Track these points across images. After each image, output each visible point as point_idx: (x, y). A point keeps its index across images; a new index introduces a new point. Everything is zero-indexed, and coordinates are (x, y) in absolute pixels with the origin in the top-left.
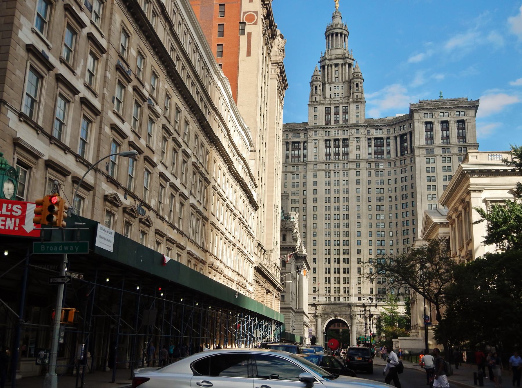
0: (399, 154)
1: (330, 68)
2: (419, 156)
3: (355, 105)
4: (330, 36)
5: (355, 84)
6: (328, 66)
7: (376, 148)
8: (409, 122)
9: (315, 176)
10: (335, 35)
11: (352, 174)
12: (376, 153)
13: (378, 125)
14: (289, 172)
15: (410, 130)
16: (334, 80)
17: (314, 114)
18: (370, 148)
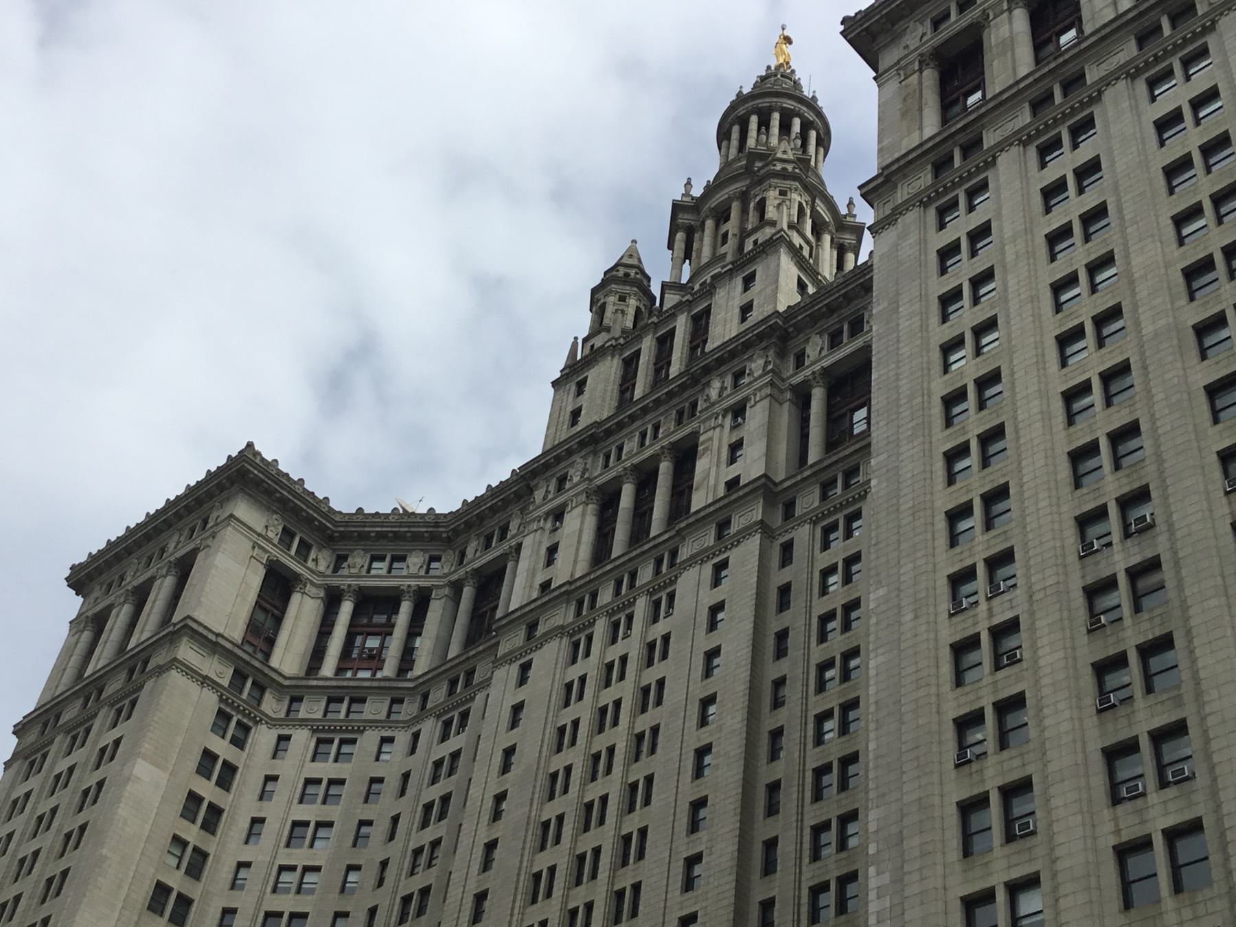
10: (736, 130)
17: (570, 409)
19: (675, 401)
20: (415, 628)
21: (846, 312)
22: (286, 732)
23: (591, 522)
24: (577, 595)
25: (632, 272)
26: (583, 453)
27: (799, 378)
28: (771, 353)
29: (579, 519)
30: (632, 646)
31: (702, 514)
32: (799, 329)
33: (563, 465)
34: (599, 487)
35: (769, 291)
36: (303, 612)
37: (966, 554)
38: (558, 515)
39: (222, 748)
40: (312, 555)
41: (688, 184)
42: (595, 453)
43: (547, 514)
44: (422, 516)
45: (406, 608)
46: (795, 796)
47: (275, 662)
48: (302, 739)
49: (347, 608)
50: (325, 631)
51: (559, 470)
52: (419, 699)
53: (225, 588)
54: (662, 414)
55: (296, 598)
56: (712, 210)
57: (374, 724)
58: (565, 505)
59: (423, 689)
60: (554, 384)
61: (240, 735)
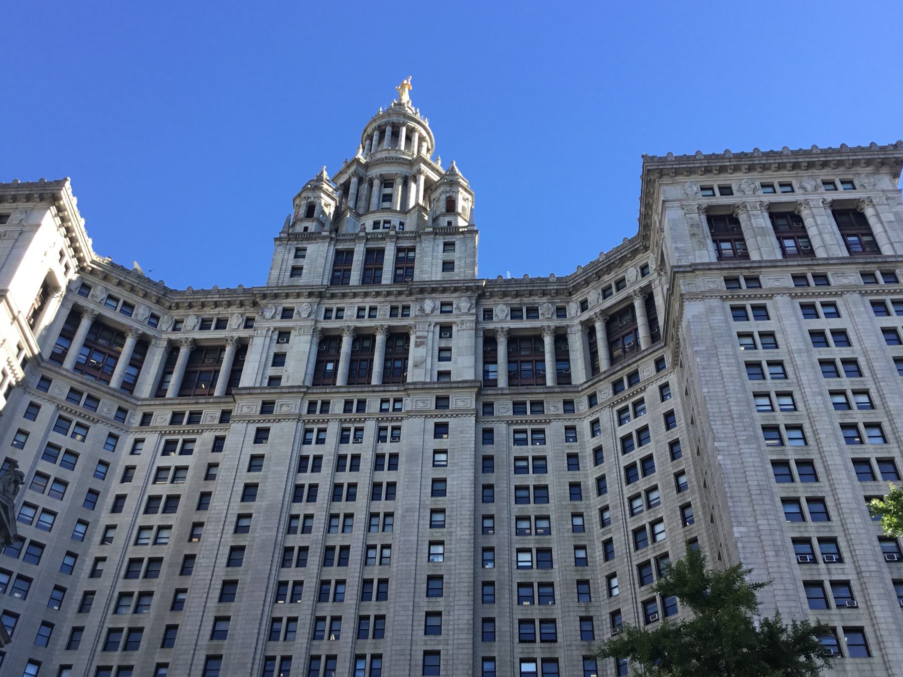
0: (603, 363)
1: (365, 186)
2: (702, 296)
3: (440, 241)
4: (376, 133)
5: (444, 197)
6: (361, 181)
7: (514, 367)
8: (640, 259)
9: (261, 435)
10: (389, 130)
11: (415, 434)
12: (512, 378)
13: (523, 293)
14: (155, 430)
15: (644, 283)
16: (373, 207)
17: (291, 262)
18: (491, 367)
19: (392, 298)
20: (137, 362)
21: (526, 300)
22: (37, 401)
24: (313, 397)
26: (310, 300)
27: (490, 326)
28: (474, 301)
29: (309, 345)
30: (366, 449)
31: (428, 386)
32: (492, 295)
33: (291, 300)
34: (323, 330)
35: (469, 260)
37: (802, 529)
38: (284, 335)
43: (275, 329)
44: (155, 284)
45: (130, 342)
46: (507, 596)
48: (47, 412)
49: (85, 324)
51: (288, 303)
54: (380, 303)
56: (381, 175)
57: (104, 420)
58: (293, 328)
59: (147, 410)
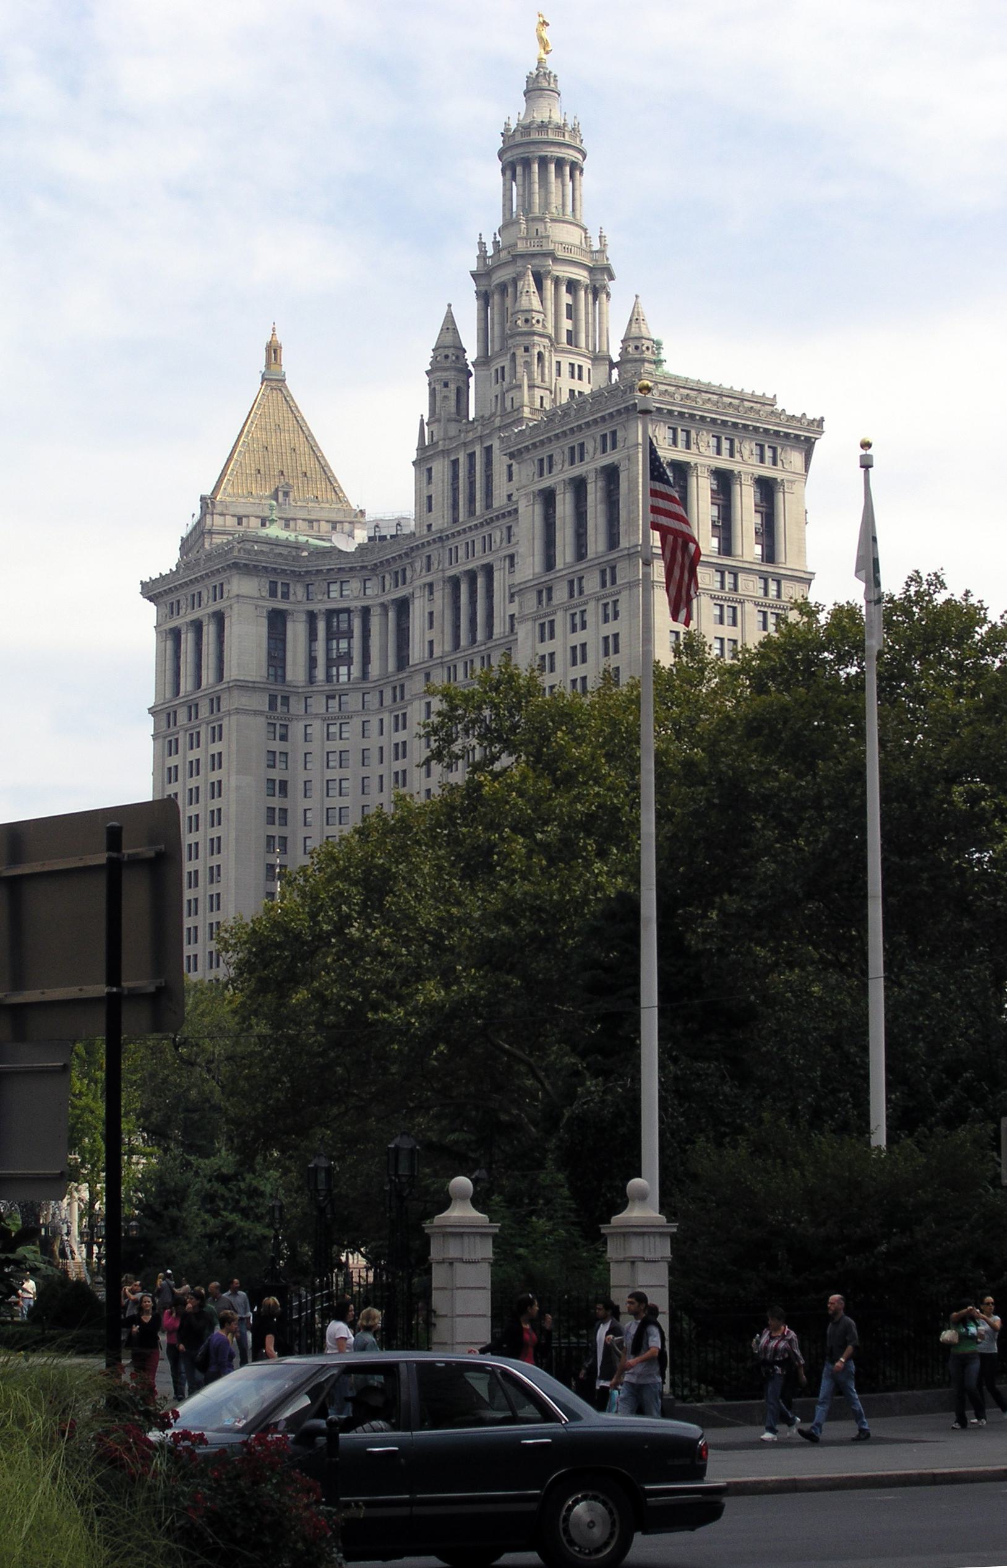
17: (425, 494)
23: (448, 600)
25: (450, 352)
36: (296, 631)
39: (277, 746)
40: (292, 591)
41: (482, 244)
42: (443, 547)
45: (357, 624)
47: (289, 677)
48: (317, 728)
49: (321, 626)
50: (312, 636)
52: (378, 694)
53: (246, 640)
55: (290, 626)
60: (414, 463)
61: (283, 731)
